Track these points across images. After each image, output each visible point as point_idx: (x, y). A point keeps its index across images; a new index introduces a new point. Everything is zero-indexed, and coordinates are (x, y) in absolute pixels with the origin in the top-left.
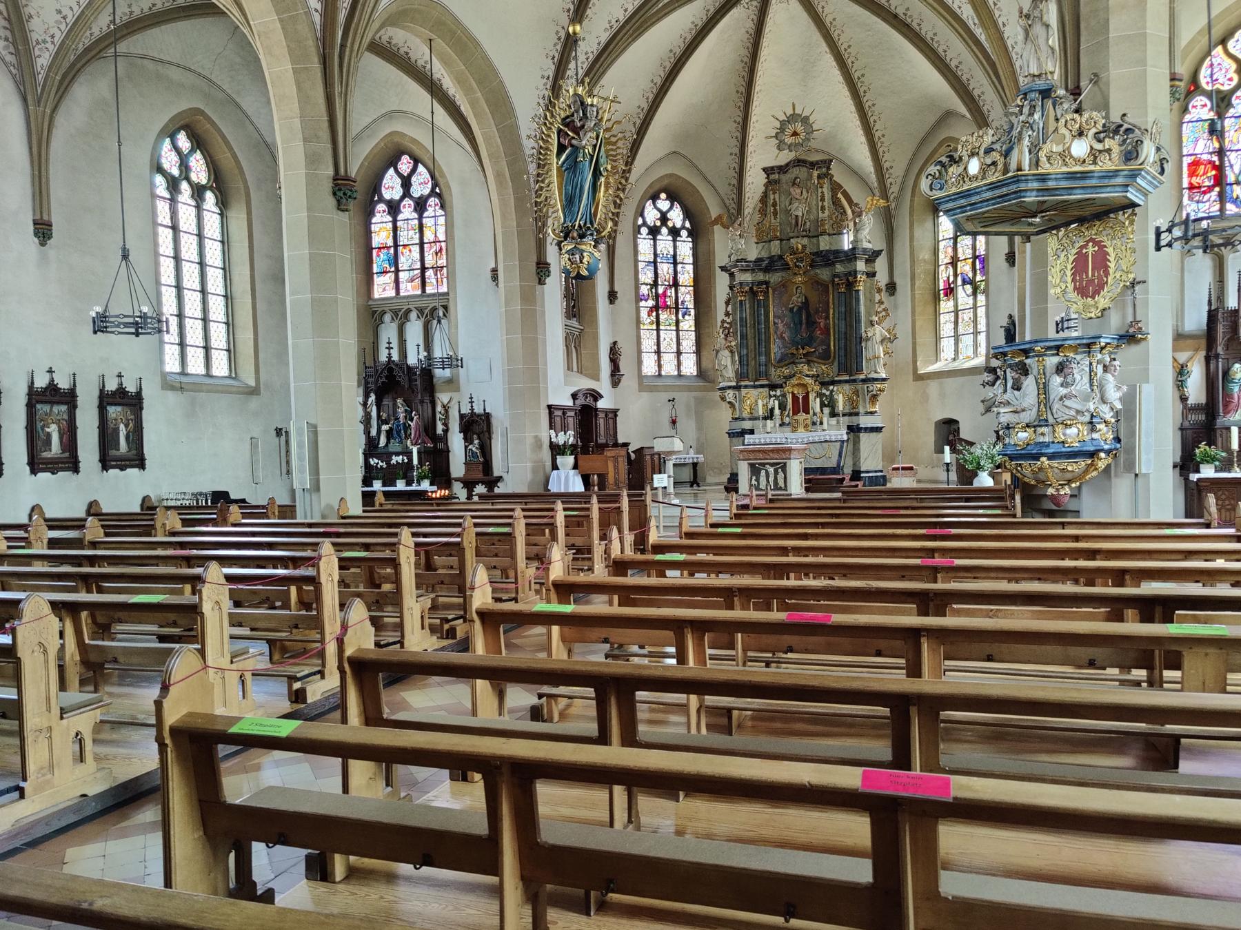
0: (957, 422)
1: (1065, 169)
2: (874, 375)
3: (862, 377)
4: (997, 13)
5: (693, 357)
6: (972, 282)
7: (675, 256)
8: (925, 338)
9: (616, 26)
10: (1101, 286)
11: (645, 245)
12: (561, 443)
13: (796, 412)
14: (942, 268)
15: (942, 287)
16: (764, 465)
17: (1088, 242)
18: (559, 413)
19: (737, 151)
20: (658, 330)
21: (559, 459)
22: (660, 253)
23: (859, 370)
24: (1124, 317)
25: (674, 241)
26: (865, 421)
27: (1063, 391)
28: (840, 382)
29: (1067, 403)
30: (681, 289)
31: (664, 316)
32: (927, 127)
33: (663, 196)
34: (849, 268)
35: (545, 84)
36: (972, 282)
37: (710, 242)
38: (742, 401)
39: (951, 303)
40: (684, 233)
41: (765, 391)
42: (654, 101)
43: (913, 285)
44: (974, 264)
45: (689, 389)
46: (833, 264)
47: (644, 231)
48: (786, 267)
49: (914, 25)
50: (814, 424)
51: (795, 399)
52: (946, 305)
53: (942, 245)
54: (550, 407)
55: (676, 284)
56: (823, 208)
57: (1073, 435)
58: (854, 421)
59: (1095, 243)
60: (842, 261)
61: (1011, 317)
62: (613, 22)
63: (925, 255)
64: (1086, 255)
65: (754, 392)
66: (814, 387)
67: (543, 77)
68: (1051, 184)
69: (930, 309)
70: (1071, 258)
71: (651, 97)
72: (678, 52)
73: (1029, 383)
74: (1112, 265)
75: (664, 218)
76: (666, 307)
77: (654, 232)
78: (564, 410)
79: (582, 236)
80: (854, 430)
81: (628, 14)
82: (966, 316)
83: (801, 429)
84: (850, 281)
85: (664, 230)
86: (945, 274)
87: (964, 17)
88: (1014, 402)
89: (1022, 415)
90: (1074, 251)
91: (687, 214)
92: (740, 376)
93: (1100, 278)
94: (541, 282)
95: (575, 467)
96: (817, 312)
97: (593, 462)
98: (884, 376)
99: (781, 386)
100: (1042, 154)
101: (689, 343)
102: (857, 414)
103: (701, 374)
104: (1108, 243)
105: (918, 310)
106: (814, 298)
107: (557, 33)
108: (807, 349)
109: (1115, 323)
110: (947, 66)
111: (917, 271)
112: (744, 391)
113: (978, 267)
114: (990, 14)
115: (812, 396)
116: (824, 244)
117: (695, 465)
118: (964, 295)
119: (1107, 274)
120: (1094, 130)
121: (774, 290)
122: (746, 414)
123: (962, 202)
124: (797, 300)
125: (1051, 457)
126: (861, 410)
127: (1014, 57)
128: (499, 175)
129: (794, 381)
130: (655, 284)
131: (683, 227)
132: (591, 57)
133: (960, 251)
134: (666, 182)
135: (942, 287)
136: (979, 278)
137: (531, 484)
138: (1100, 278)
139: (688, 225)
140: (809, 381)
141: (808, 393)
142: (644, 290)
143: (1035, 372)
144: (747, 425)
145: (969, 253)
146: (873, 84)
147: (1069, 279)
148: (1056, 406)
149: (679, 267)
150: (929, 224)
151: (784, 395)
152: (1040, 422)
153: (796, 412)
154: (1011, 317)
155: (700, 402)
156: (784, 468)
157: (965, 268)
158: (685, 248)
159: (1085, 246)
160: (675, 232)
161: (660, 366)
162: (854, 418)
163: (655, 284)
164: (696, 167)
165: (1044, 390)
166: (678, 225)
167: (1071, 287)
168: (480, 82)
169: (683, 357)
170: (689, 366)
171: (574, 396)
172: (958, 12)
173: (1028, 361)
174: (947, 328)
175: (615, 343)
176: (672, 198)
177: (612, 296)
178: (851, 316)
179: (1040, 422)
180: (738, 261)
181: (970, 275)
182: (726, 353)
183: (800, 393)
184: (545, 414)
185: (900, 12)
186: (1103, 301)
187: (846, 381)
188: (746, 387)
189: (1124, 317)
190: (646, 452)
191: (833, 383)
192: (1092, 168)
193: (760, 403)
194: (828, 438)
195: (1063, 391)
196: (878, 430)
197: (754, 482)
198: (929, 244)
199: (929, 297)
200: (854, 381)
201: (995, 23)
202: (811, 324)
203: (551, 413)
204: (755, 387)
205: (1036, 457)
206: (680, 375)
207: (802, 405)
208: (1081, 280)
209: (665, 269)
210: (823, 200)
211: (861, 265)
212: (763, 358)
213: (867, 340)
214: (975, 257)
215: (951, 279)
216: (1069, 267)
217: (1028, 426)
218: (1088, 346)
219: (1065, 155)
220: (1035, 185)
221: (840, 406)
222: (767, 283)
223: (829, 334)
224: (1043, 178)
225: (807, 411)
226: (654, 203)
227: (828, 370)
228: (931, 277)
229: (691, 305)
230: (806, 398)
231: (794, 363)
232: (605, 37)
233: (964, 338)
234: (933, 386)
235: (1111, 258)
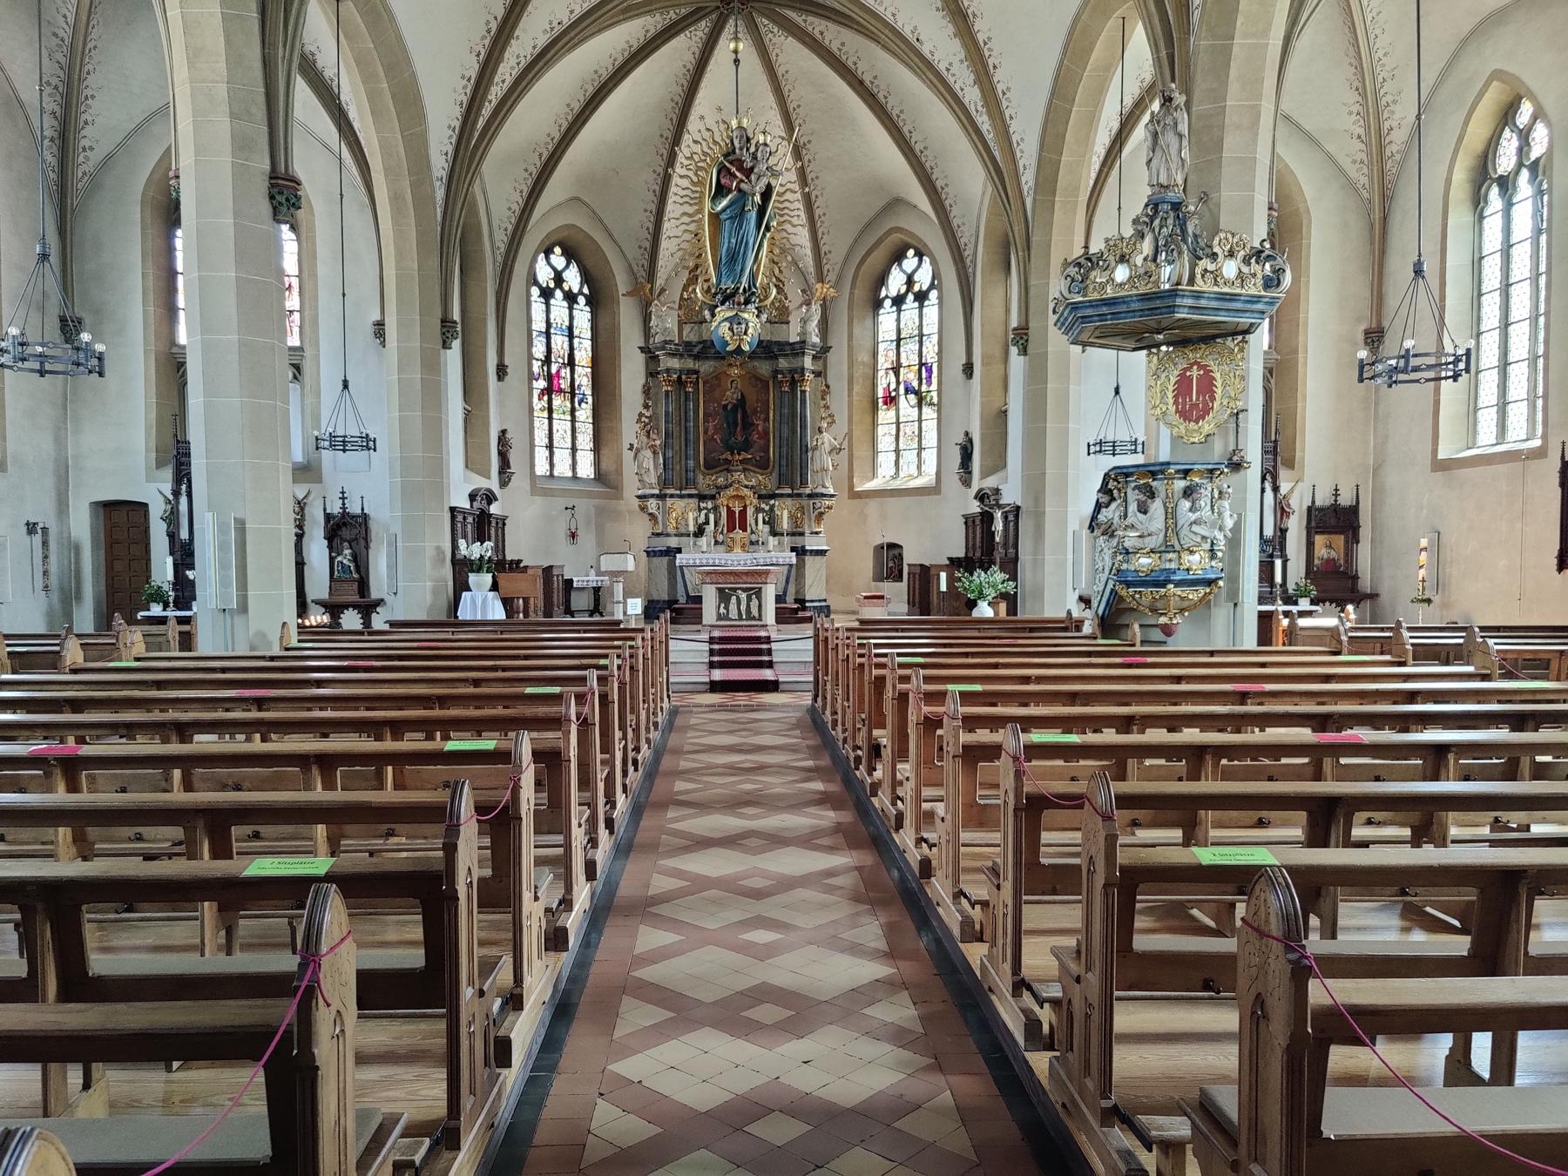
1: (1216, 289)
2: (824, 491)
3: (808, 491)
4: (1005, 104)
5: (590, 456)
6: (917, 393)
7: (570, 328)
8: (861, 451)
9: (558, 29)
10: (1207, 410)
11: (538, 308)
12: (476, 556)
13: (731, 528)
14: (881, 373)
15: (880, 394)
16: (735, 590)
17: (1192, 365)
18: (460, 518)
19: (653, 207)
20: (550, 418)
21: (473, 578)
22: (555, 321)
23: (804, 483)
24: (1226, 445)
25: (571, 309)
26: (811, 544)
27: (1193, 516)
28: (782, 495)
29: (1195, 528)
30: (578, 370)
31: (557, 401)
33: (558, 250)
34: (795, 363)
35: (465, 87)
36: (917, 393)
37: (615, 315)
38: (667, 513)
39: (892, 413)
40: (582, 300)
41: (693, 502)
42: (568, 130)
43: (850, 390)
44: (920, 371)
45: (590, 495)
46: (776, 357)
47: (535, 291)
49: (881, 96)
50: (752, 543)
51: (730, 513)
52: (886, 416)
53: (881, 347)
54: (453, 510)
55: (571, 363)
57: (1196, 562)
58: (798, 541)
59: (1201, 367)
61: (967, 434)
62: (555, 24)
63: (863, 357)
64: (1190, 379)
65: (679, 504)
67: (463, 77)
68: (1203, 303)
69: (869, 419)
70: (1173, 380)
71: (565, 125)
72: (605, 76)
73: (1156, 507)
74: (1219, 391)
75: (559, 278)
76: (560, 391)
77: (547, 294)
78: (464, 512)
79: (747, 302)
80: (800, 552)
81: (574, 17)
82: (909, 429)
83: (738, 549)
84: (795, 377)
85: (559, 294)
86: (885, 381)
87: (966, 101)
88: (1139, 526)
89: (1147, 540)
90: (1177, 373)
91: (586, 277)
92: (665, 482)
93: (1205, 403)
94: (446, 345)
95: (495, 587)
96: (755, 412)
97: (508, 581)
98: (832, 491)
99: (713, 497)
100: (1198, 271)
101: (585, 440)
102: (802, 534)
103: (600, 476)
104: (1215, 368)
105: (855, 418)
106: (751, 397)
107: (488, 22)
108: (745, 455)
109: (1218, 451)
110: (911, 149)
111: (856, 375)
112: (669, 501)
114: (998, 104)
115: (750, 511)
117: (597, 590)
118: (907, 405)
119: (1213, 399)
120: (1242, 253)
122: (671, 530)
123: (1105, 310)
124: (731, 396)
125: (1178, 584)
126: (807, 532)
127: (1019, 154)
128: (396, 199)
129: (731, 492)
130: (547, 361)
131: (581, 293)
132: (523, 64)
133: (903, 355)
134: (566, 233)
135: (880, 394)
136: (924, 388)
137: (431, 608)
138: (1205, 403)
139: (586, 290)
140: (746, 492)
142: (536, 366)
143: (1163, 494)
144: (673, 542)
146: (819, 152)
147: (1171, 401)
148: (1184, 532)
149: (576, 341)
150: (869, 322)
151: (715, 508)
152: (1167, 548)
153: (731, 528)
154: (967, 434)
155: (600, 512)
156: (759, 593)
157: (909, 376)
158: (583, 317)
159: (1189, 368)
160: (571, 298)
161: (552, 465)
163: (547, 361)
164: (601, 221)
165: (1171, 514)
166: (575, 290)
167: (1172, 409)
168: (389, 69)
169: (579, 454)
170: (586, 469)
171: (472, 497)
172: (960, 94)
173: (1154, 484)
174: (885, 441)
175: (504, 432)
176: (569, 255)
177: (502, 371)
178: (793, 419)
179: (1167, 548)
180: (666, 342)
181: (915, 384)
182: (648, 453)
184: (447, 516)
185: (867, 79)
186: (1207, 426)
187: (789, 496)
188: (672, 496)
189: (1226, 445)
190: (555, 572)
191: (773, 496)
192: (1238, 291)
193: (691, 516)
195: (1193, 516)
196: (822, 553)
197: (722, 610)
198: (869, 344)
199: (867, 405)
200: (799, 495)
201: (1001, 114)
202: (748, 425)
203: (453, 518)
204: (681, 496)
205: (1163, 584)
206: (575, 477)
207: (737, 521)
208: (1184, 403)
209: (559, 342)
211: (808, 362)
212: (691, 463)
213: (815, 448)
214: (921, 364)
216: (1171, 388)
217: (1152, 551)
218: (1211, 471)
219: (1216, 276)
220: (1189, 302)
221: (785, 524)
222: (696, 372)
224: (1198, 295)
225: (745, 530)
226: (547, 258)
227: (767, 481)
228: (869, 383)
229: (588, 392)
230: (743, 513)
231: (728, 471)
232: (542, 41)
234: (872, 506)
235: (1219, 383)
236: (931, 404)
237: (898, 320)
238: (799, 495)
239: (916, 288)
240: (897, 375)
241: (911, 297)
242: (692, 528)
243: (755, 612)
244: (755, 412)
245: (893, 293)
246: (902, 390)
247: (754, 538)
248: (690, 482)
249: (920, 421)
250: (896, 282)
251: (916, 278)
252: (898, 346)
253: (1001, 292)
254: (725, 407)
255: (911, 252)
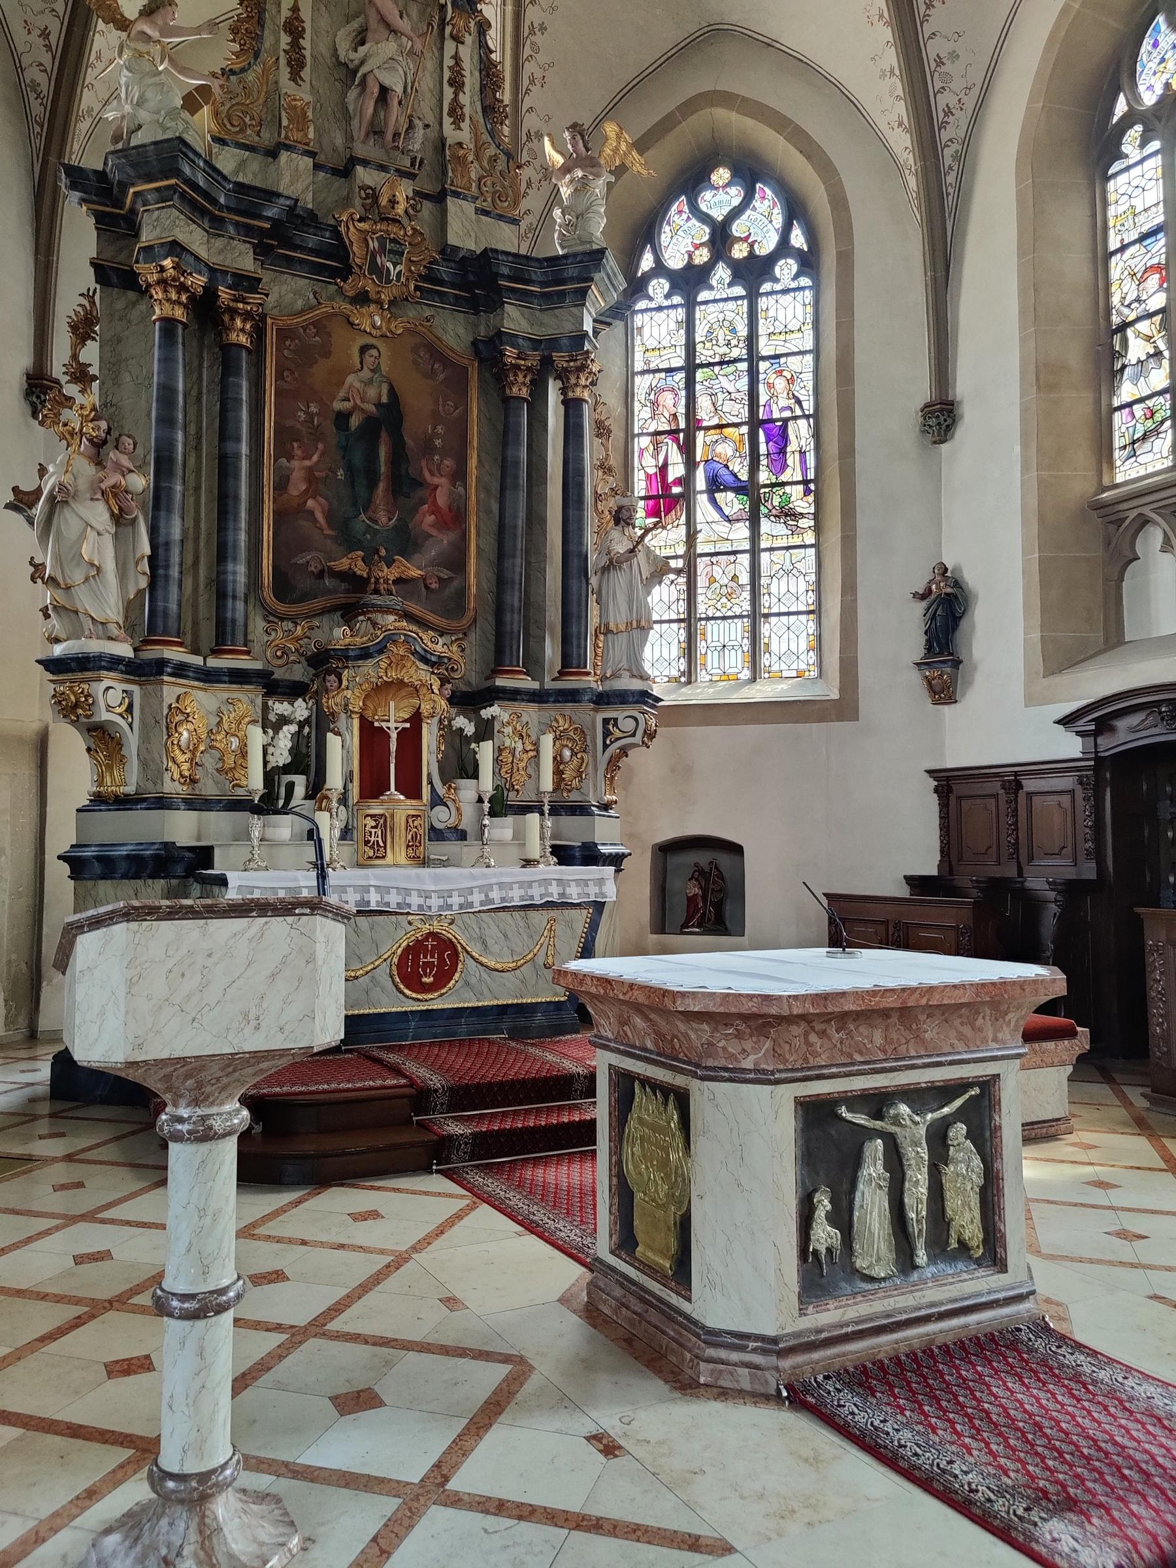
0: (736, 850)
2: (628, 684)
13: (373, 787)
15: (640, 487)
16: (877, 1103)
23: (571, 661)
32: (648, 57)
34: (554, 324)
36: (748, 489)
41: (247, 699)
46: (493, 302)
48: (334, 262)
50: (437, 834)
51: (372, 736)
56: (456, 111)
58: (573, 830)
60: (524, 296)
65: (203, 702)
66: (435, 703)
83: (398, 853)
92: (150, 620)
96: (428, 449)
106: (419, 400)
112: (171, 690)
113: (763, 449)
116: (466, 229)
121: (284, 334)
122: (171, 786)
124: (360, 391)
129: (370, 671)
133: (703, 404)
135: (640, 487)
136: (764, 476)
141: (416, 719)
144: (182, 829)
145: (738, 411)
153: (373, 787)
162: (567, 821)
182: (99, 514)
183: (393, 719)
188: (181, 670)
194: (554, 893)
197: (824, 1235)
200: (572, 696)
202: (406, 484)
204: (208, 677)
210: (457, 83)
212: (239, 572)
214: (755, 423)
215: (676, 470)
223: (464, 536)
225: (411, 789)
233: (714, 633)
236: (787, 514)
237: (689, 325)
238: (572, 696)
239: (739, 252)
240: (688, 450)
241: (722, 273)
242: (256, 782)
243: (966, 1221)
244: (428, 449)
245: (675, 261)
246: (701, 483)
247: (442, 817)
248: (224, 636)
249: (754, 552)
250: (681, 240)
251: (737, 229)
252: (690, 384)
253: (1070, 222)
254: (342, 418)
255: (721, 175)
